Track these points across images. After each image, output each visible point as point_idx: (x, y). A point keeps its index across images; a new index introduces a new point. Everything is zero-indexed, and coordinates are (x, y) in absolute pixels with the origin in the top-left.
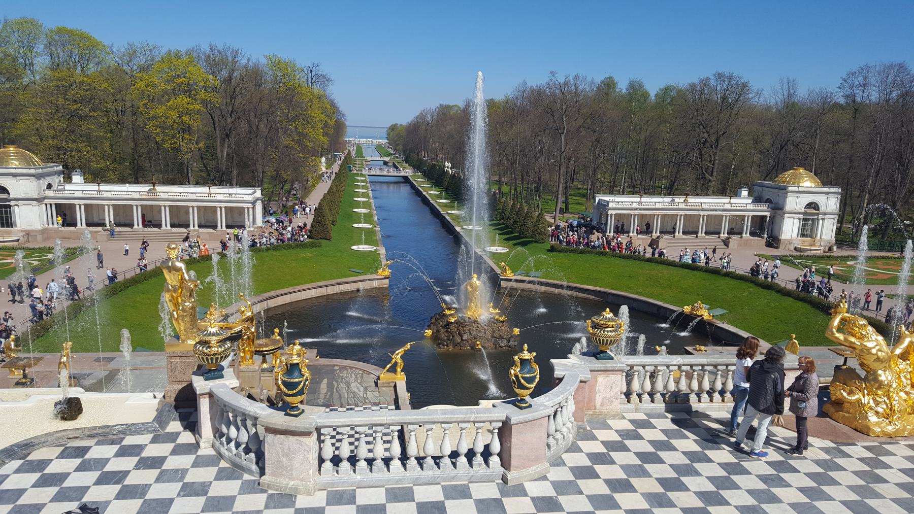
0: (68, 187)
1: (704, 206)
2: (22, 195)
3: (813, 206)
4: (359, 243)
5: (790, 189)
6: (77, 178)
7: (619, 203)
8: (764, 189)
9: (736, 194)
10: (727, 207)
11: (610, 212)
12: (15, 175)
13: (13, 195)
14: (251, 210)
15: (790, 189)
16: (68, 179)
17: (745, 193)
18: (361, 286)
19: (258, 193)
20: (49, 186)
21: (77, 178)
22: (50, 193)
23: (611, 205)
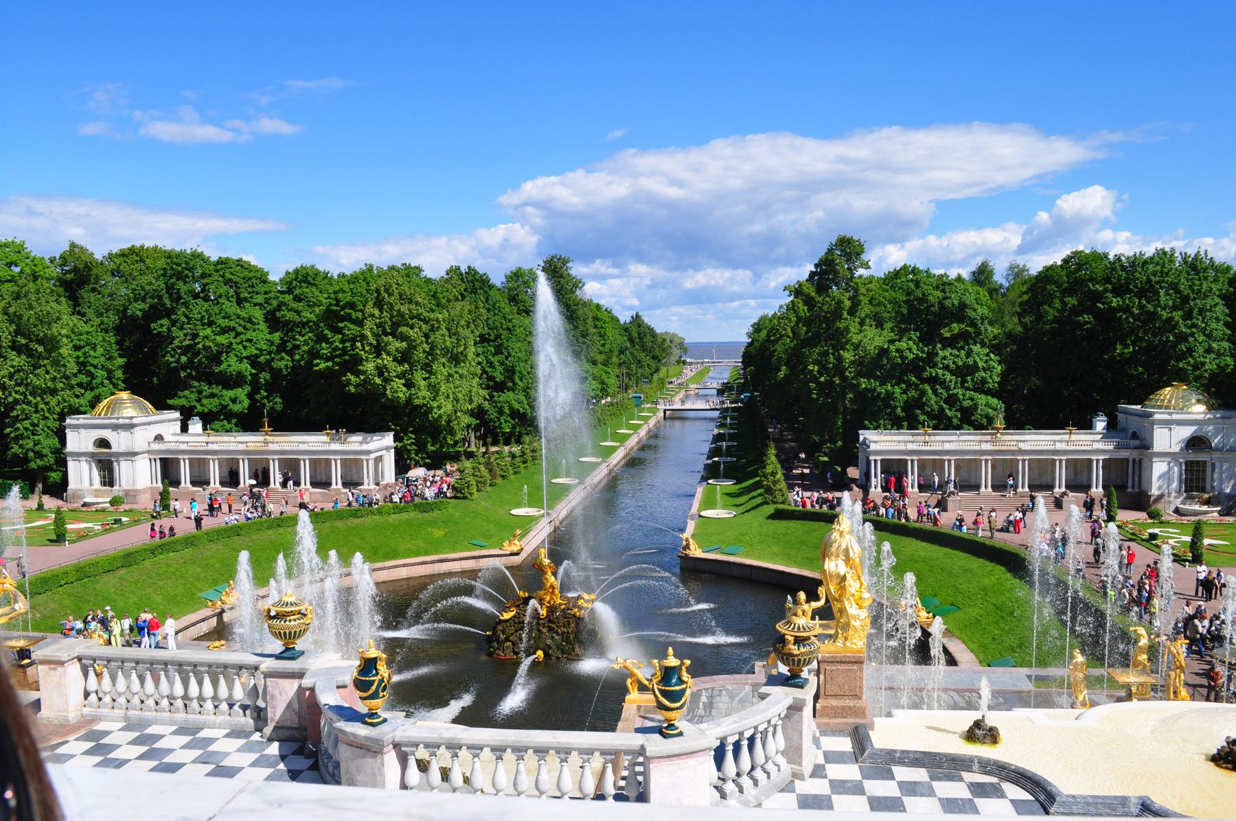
0: (184, 438)
1: (1023, 446)
2: (122, 449)
3: (1195, 443)
4: (519, 505)
5: (1157, 417)
6: (196, 426)
7: (881, 442)
8: (1130, 417)
9: (1087, 425)
10: (1059, 446)
11: (872, 458)
12: (115, 427)
13: (115, 449)
14: (371, 463)
15: (1157, 417)
16: (184, 429)
17: (1100, 424)
18: (484, 563)
19: (388, 439)
20: (159, 438)
21: (196, 426)
22: (156, 446)
23: (873, 447)
